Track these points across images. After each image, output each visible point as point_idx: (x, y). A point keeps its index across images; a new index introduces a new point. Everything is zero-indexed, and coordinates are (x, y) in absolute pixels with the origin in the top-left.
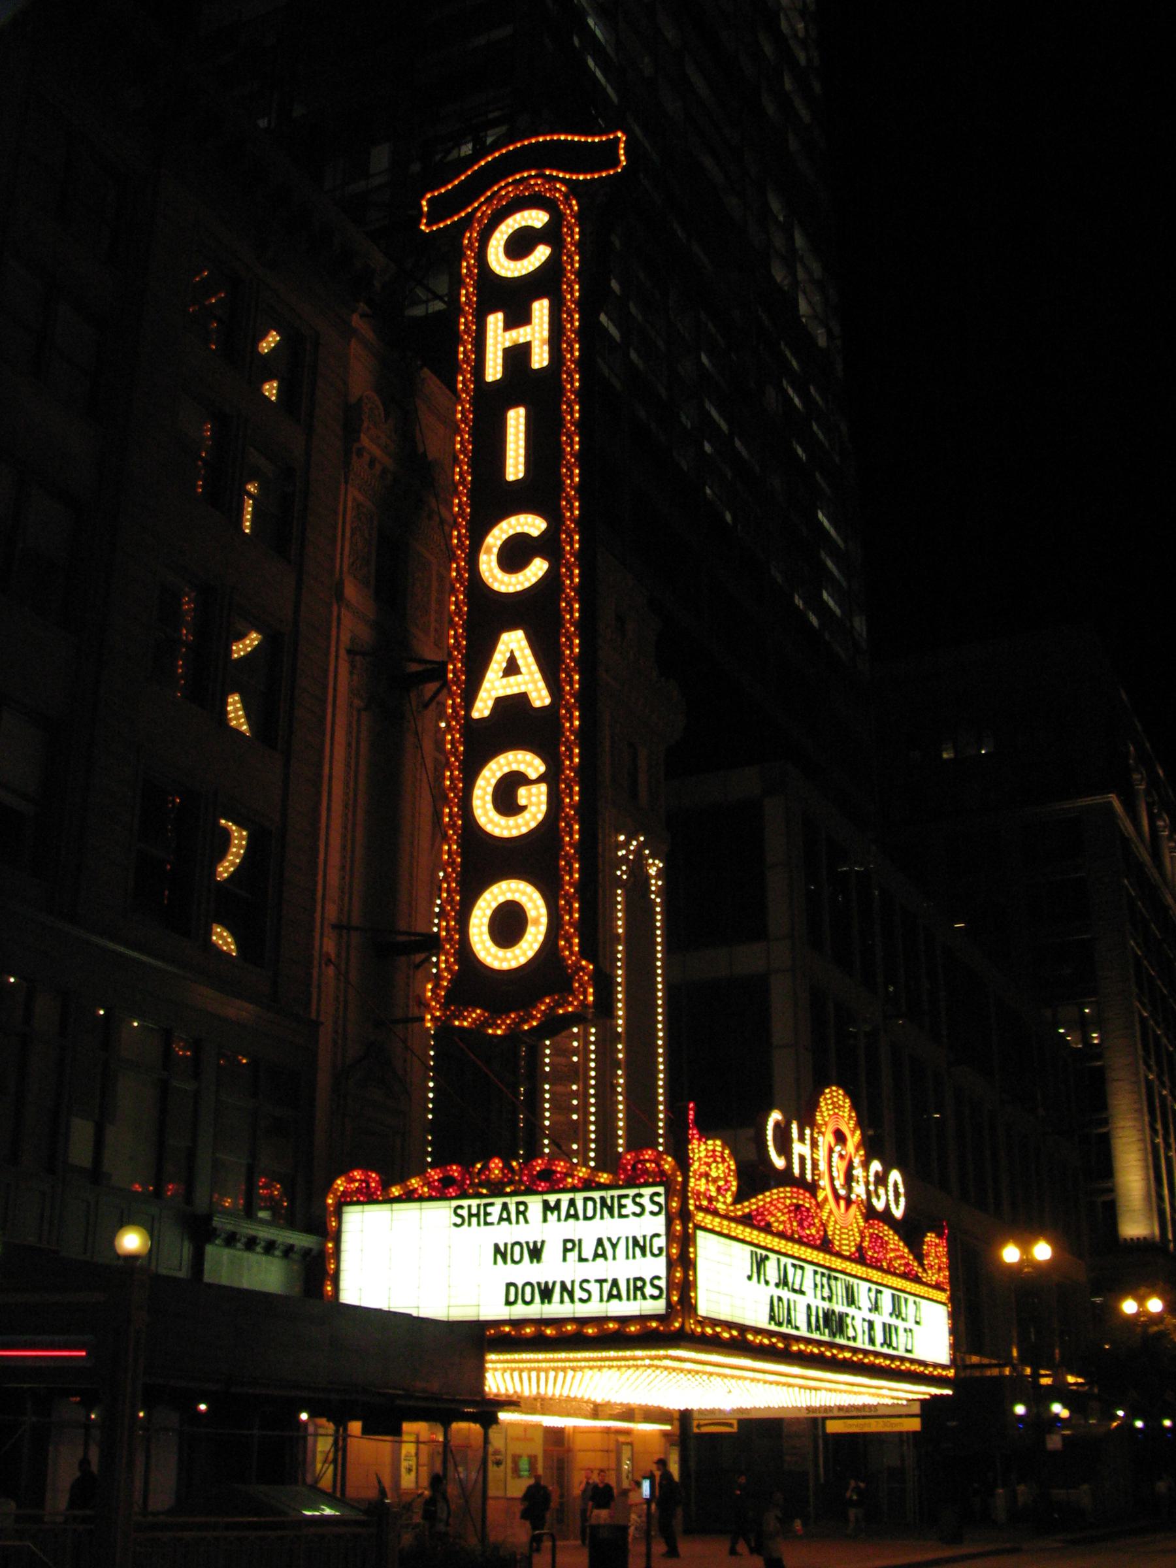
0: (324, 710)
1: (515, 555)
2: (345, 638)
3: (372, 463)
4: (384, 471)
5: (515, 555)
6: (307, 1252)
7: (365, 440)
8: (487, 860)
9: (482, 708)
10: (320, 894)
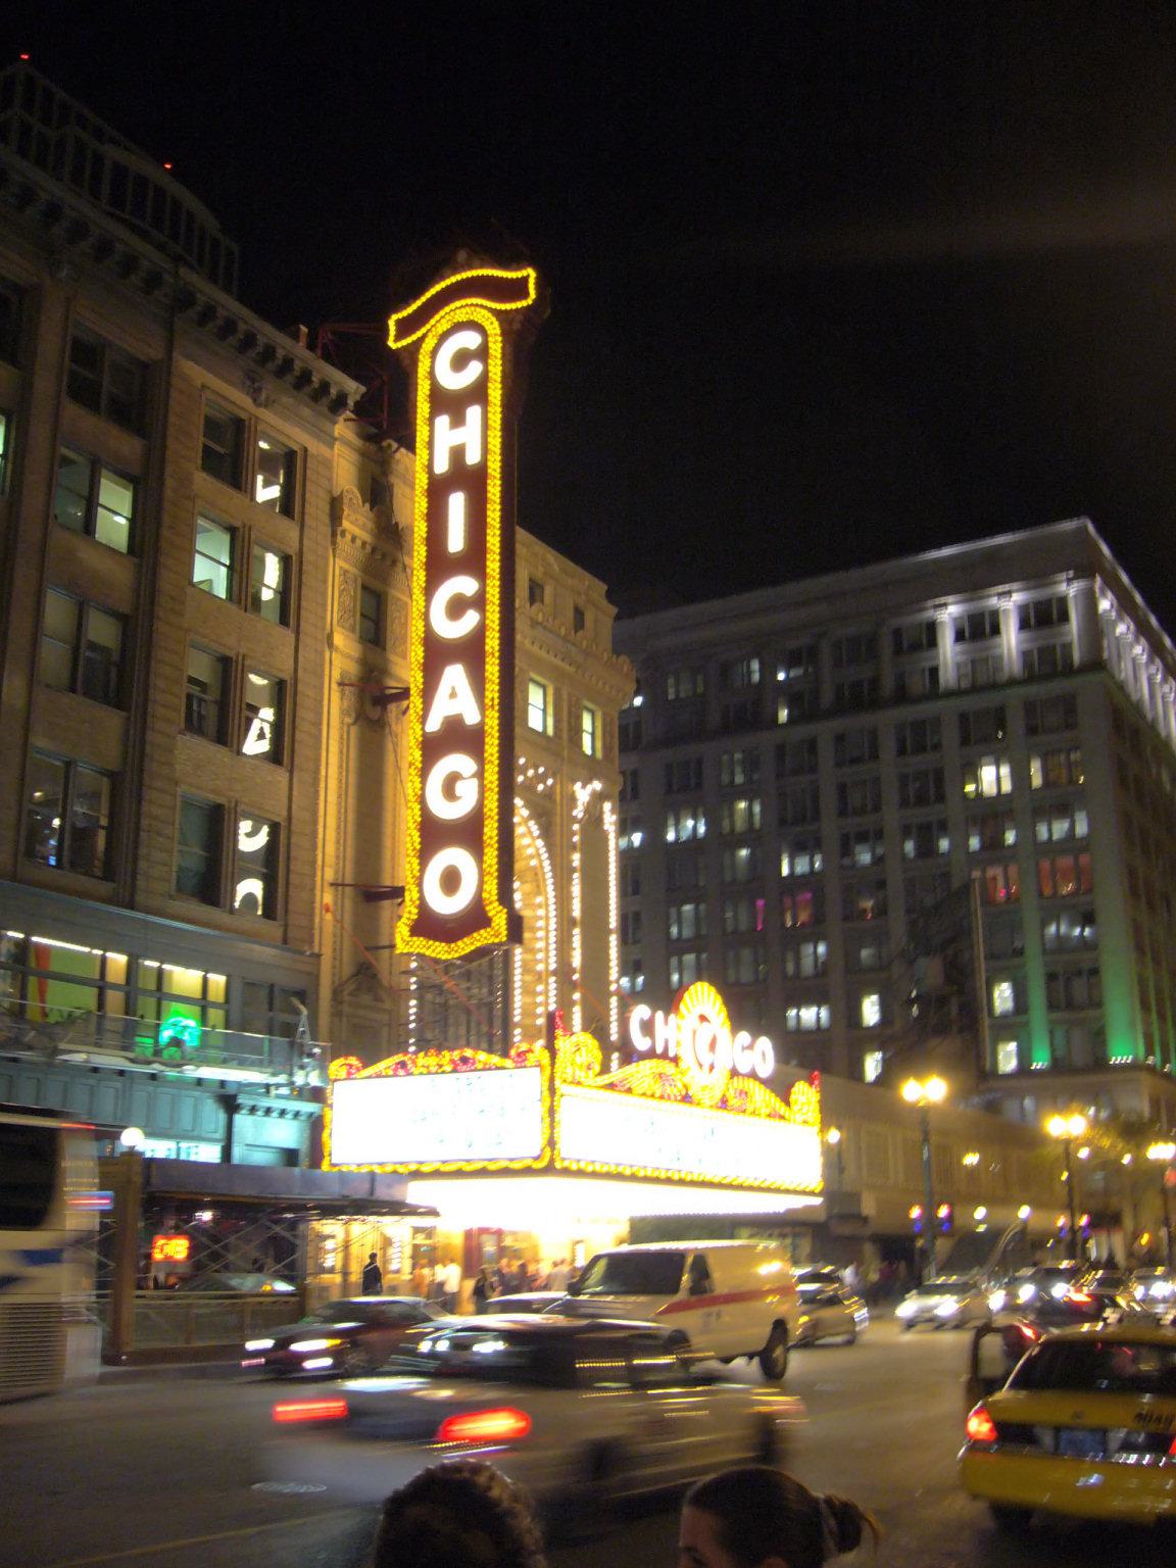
0: (320, 731)
1: (457, 607)
2: (336, 675)
3: (354, 539)
4: (364, 544)
5: (457, 607)
6: (311, 1114)
7: (346, 524)
8: (434, 834)
9: (434, 724)
10: (319, 862)
